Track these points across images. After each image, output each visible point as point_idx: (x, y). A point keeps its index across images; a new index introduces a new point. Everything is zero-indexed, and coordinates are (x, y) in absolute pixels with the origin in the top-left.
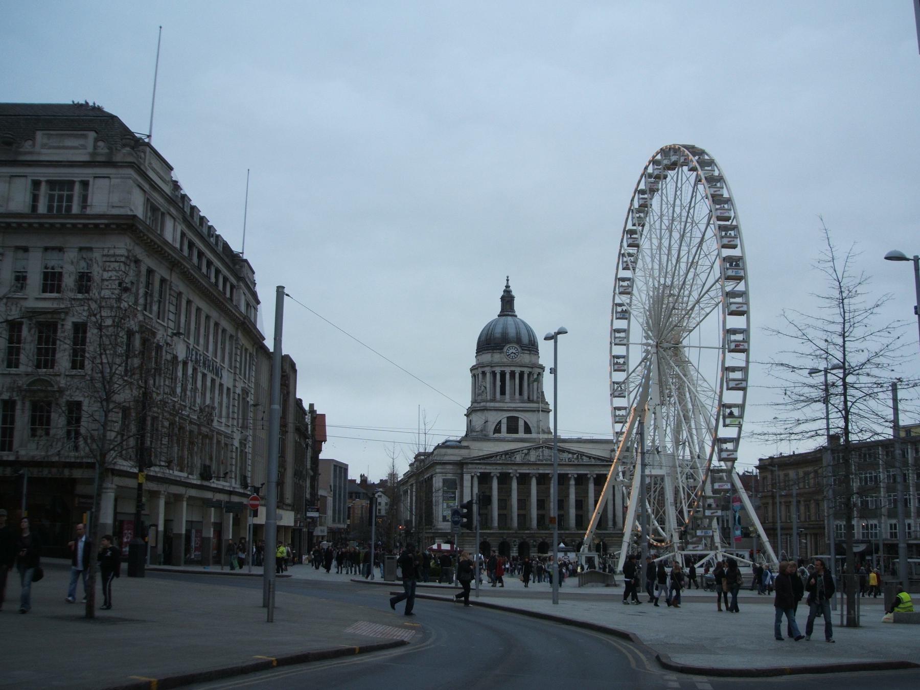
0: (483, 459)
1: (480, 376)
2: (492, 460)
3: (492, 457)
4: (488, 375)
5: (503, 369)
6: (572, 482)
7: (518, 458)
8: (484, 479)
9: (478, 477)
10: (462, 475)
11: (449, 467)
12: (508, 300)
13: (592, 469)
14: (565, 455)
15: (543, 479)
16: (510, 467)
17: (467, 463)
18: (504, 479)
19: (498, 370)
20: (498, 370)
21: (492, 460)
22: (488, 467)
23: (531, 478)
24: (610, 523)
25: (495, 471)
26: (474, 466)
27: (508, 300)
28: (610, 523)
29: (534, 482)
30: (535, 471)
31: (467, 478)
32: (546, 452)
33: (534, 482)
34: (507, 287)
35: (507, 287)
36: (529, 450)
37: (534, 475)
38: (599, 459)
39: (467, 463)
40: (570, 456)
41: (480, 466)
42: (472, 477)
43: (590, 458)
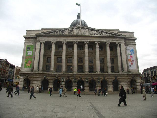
3: (52, 33)
6: (97, 46)
7: (67, 33)
8: (48, 45)
9: (44, 43)
10: (35, 43)
11: (32, 40)
12: (79, 16)
13: (108, 39)
14: (93, 32)
15: (81, 45)
18: (59, 45)
21: (52, 34)
22: (50, 38)
24: (120, 69)
26: (43, 38)
27: (79, 16)
28: (120, 69)
29: (75, 46)
30: (76, 40)
31: (38, 44)
32: (82, 30)
33: (75, 46)
34: (79, 13)
35: (79, 13)
36: (73, 29)
37: (76, 42)
38: (111, 34)
40: (96, 32)
42: (41, 43)
43: (106, 33)
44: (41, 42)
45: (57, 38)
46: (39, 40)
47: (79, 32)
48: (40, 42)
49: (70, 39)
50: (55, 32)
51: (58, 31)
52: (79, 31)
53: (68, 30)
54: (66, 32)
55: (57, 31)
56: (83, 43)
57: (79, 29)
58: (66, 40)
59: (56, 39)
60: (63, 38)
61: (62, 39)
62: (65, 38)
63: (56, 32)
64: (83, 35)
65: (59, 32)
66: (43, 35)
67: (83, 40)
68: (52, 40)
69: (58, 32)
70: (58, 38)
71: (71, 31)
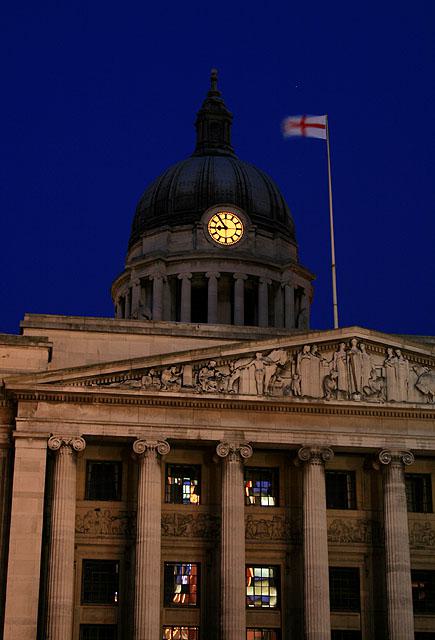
0: (103, 380)
1: (137, 292)
2: (142, 388)
4: (157, 285)
5: (199, 268)
8: (109, 472)
16: (214, 417)
17: (31, 397)
19: (185, 271)
20: (185, 271)
22: (120, 416)
23: (304, 466)
25: (149, 429)
26: (62, 408)
30: (321, 440)
36: (295, 352)
37: (321, 456)
39: (31, 397)
41: (89, 412)
42: (52, 456)
44: (55, 444)
45: (177, 421)
46: (40, 426)
47: (343, 374)
48: (43, 444)
49: (279, 431)
50: (159, 371)
51: (187, 363)
52: (341, 364)
53: (259, 364)
54: (244, 374)
55: (180, 366)
56: (369, 457)
57: (342, 353)
58: (251, 437)
59: (169, 421)
60: (225, 423)
61: (217, 430)
62: (236, 422)
63: (169, 367)
64: (375, 402)
65: (196, 371)
66: (66, 389)
67: (369, 443)
68: (136, 432)
69: (188, 373)
70: (188, 422)
71: (282, 368)
